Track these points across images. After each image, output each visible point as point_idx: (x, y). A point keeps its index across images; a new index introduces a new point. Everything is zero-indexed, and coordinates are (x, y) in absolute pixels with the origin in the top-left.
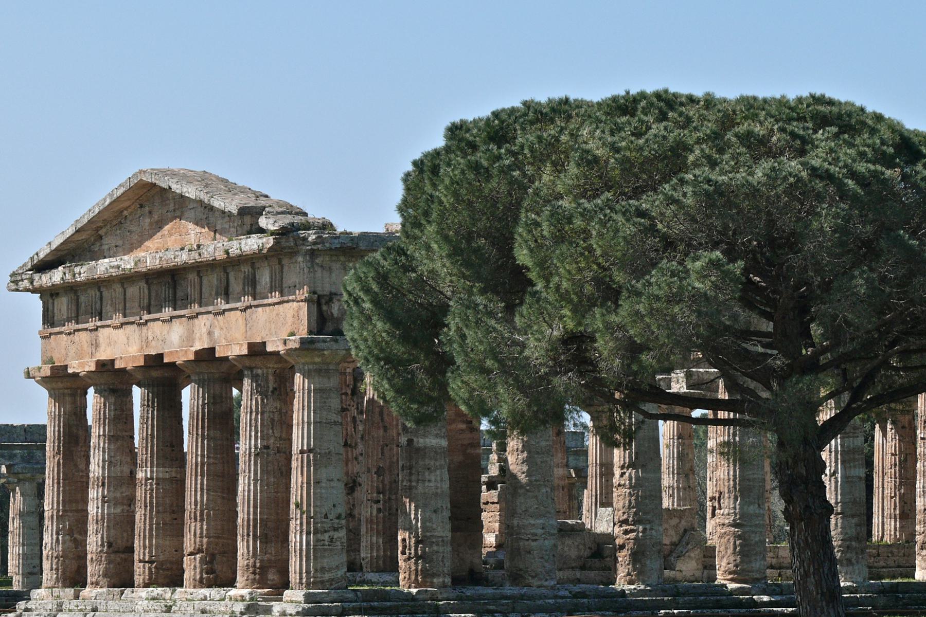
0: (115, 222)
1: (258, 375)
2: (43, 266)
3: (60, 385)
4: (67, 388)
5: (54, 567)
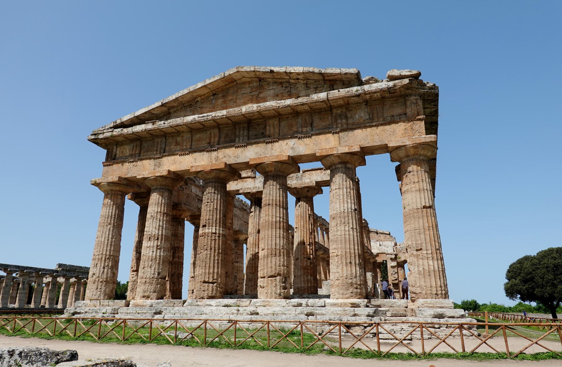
0: (187, 104)
1: (349, 168)
2: (123, 125)
3: (118, 188)
4: (119, 191)
5: (99, 287)
